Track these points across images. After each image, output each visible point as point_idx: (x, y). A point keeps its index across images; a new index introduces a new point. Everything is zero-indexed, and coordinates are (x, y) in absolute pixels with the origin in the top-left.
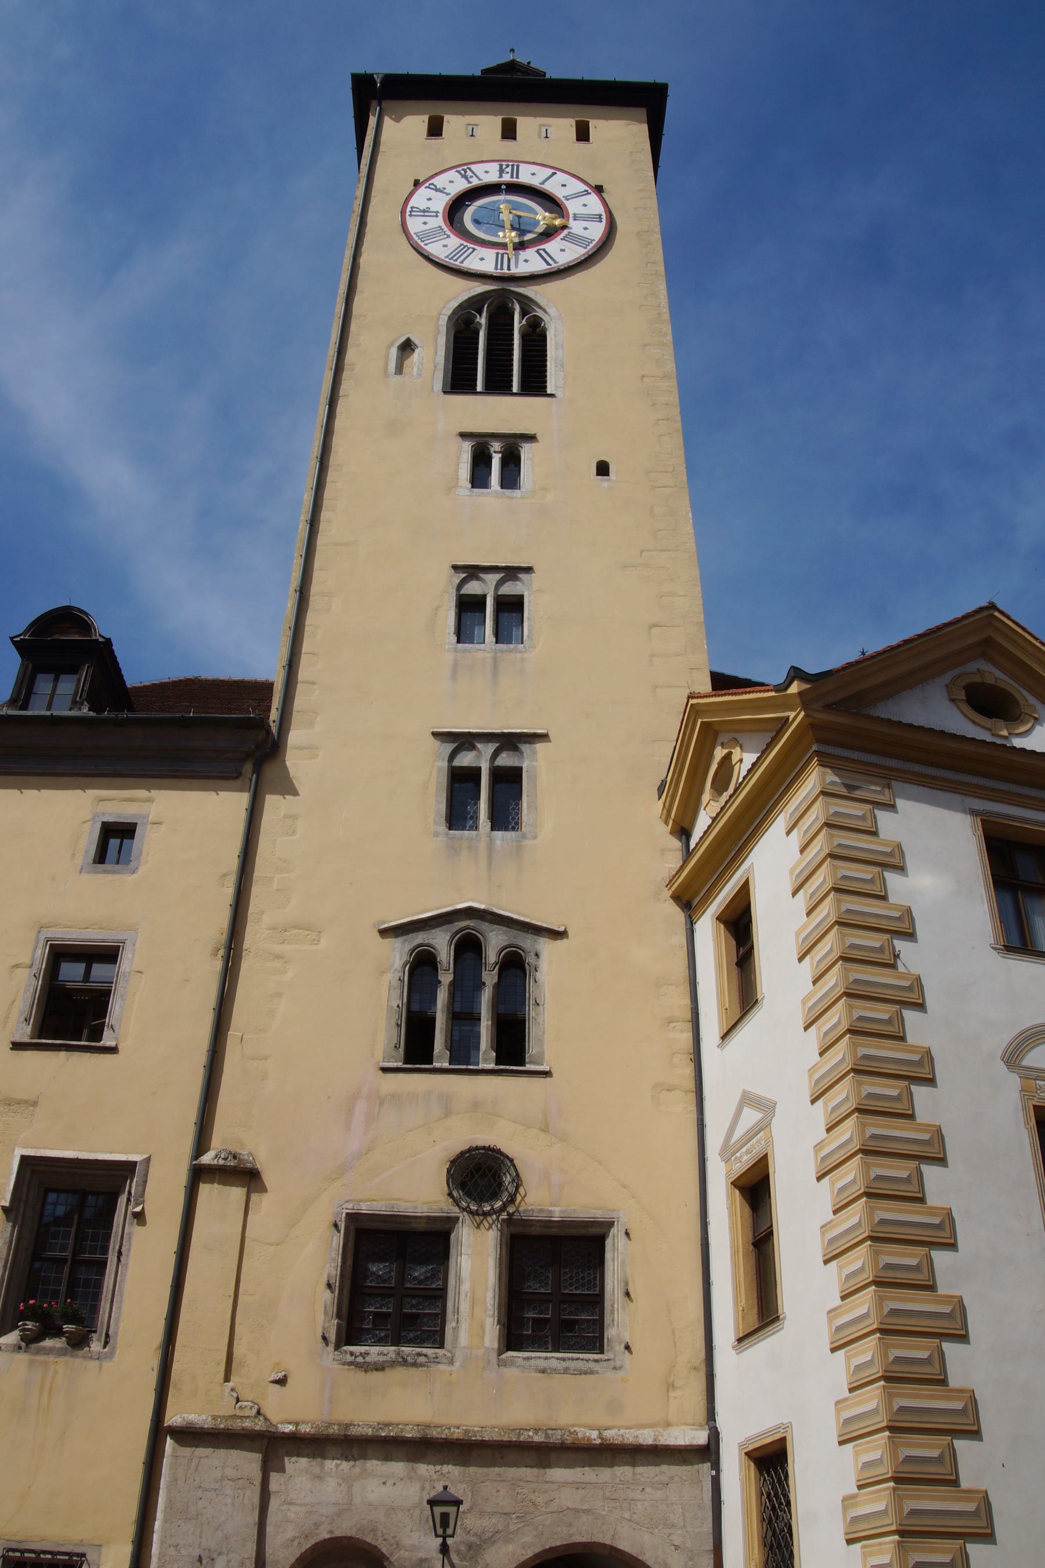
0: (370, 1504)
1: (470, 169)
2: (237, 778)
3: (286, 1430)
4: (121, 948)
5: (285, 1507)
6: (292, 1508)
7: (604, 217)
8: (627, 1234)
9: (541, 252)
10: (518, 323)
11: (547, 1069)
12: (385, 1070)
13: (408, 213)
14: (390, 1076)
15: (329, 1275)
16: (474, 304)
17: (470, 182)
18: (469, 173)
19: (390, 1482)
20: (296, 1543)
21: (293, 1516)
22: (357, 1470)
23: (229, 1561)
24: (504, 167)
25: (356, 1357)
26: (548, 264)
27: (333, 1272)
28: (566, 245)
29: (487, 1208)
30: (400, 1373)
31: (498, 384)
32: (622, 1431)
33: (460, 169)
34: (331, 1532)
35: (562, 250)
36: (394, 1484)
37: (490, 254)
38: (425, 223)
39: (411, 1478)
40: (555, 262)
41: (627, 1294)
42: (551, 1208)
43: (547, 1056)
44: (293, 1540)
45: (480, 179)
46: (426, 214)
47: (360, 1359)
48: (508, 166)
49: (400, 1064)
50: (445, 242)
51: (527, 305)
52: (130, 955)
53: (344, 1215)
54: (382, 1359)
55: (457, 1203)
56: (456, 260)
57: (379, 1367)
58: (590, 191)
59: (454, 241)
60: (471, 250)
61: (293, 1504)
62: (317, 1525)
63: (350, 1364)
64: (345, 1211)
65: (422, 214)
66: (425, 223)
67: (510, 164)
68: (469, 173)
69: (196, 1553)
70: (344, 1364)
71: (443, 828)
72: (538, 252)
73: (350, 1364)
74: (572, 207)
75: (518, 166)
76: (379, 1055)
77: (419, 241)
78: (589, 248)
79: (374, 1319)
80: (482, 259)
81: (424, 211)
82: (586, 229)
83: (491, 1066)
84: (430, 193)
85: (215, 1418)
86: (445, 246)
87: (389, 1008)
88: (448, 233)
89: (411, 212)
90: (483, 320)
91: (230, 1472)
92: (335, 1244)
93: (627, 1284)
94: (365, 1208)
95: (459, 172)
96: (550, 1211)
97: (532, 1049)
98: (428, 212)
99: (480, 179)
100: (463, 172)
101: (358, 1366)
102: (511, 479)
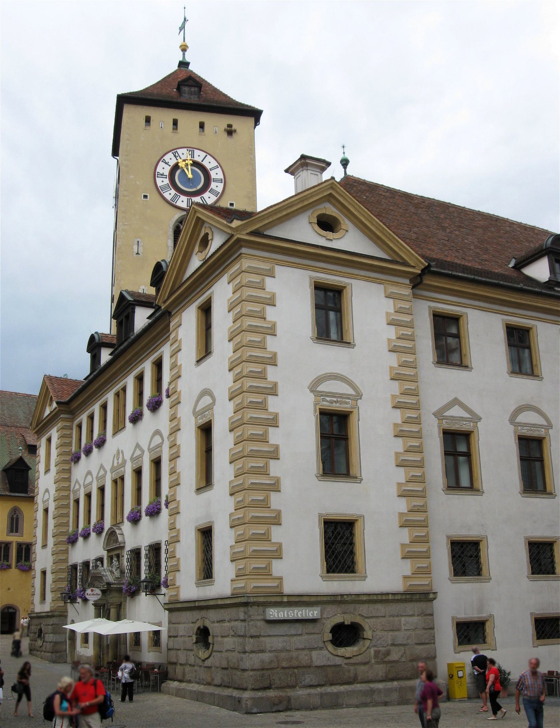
1: (177, 152)
7: (223, 180)
17: (177, 160)
33: (173, 152)
35: (209, 198)
38: (163, 181)
59: (173, 192)
66: (163, 181)
67: (191, 149)
68: (177, 155)
72: (201, 198)
74: (213, 174)
75: (194, 151)
78: (218, 196)
81: (162, 175)
88: (171, 187)
89: (158, 175)
95: (173, 153)
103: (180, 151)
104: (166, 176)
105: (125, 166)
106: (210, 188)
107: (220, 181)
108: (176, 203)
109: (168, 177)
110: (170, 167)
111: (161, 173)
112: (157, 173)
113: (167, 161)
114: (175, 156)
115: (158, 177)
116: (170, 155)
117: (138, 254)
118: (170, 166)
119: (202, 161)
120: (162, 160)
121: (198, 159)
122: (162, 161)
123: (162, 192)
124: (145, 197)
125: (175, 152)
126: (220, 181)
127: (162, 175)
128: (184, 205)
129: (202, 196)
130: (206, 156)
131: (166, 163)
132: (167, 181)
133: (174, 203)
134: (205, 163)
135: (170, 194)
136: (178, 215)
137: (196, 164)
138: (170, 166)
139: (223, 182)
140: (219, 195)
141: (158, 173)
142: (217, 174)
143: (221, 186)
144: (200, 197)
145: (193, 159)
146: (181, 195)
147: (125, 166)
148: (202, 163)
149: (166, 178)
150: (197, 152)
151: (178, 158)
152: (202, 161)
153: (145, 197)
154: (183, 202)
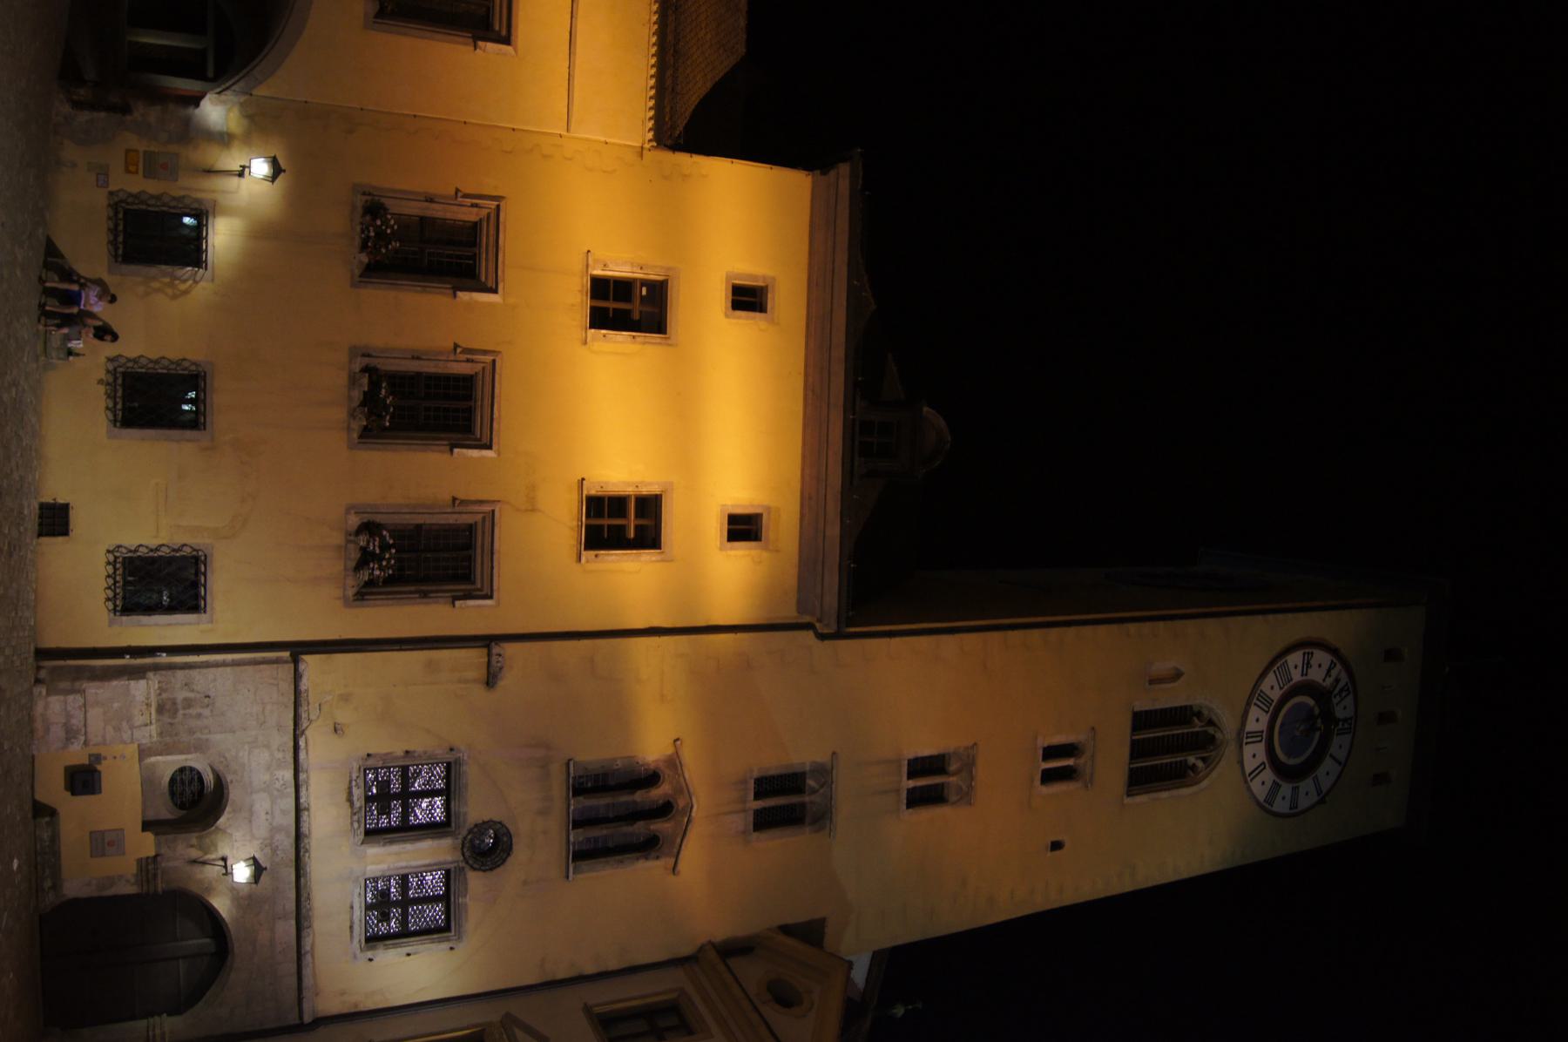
0: (252, 806)
1: (1349, 693)
2: (799, 613)
3: (300, 743)
4: (658, 551)
5: (246, 747)
6: (247, 753)
8: (452, 948)
9: (1263, 767)
11: (570, 878)
12: (568, 765)
14: (564, 769)
15: (414, 752)
18: (1344, 694)
19: (269, 817)
20: (222, 759)
21: (241, 754)
22: (275, 793)
23: (207, 718)
24: (1349, 721)
25: (356, 781)
26: (1250, 775)
27: (416, 755)
28: (1269, 784)
29: (467, 854)
30: (346, 810)
31: (1137, 750)
32: (311, 965)
34: (232, 782)
35: (1263, 783)
36: (267, 820)
37: (1263, 725)
38: (1296, 667)
39: (271, 830)
40: (1251, 780)
41: (409, 955)
42: (468, 897)
43: (579, 876)
44: (224, 757)
45: (1337, 704)
47: (354, 783)
48: (1350, 724)
49: (572, 775)
50: (1276, 687)
52: (654, 558)
53: (458, 755)
54: (355, 798)
55: (470, 831)
56: (1258, 699)
57: (350, 800)
58: (1321, 795)
59: (1276, 695)
60: (1266, 709)
61: (249, 754)
62: (235, 772)
63: (350, 776)
64: (461, 755)
65: (1306, 661)
66: (1296, 667)
68: (1344, 694)
69: (210, 694)
70: (350, 773)
71: (756, 774)
72: (1263, 763)
73: (350, 776)
74: (1307, 785)
76: (578, 758)
77: (1279, 665)
79: (385, 781)
80: (1257, 720)
81: (1308, 663)
82: (1284, 798)
83: (572, 839)
84: (1325, 667)
85: (307, 691)
86: (1272, 688)
87: (615, 760)
91: (269, 707)
92: (437, 752)
93: (415, 953)
94: (464, 768)
96: (465, 896)
97: (584, 864)
98: (1307, 667)
99: (1337, 704)
100: (1346, 688)
101: (351, 782)
102: (1049, 777)
103: (1349, 700)
108: (1255, 704)
109: (1304, 678)
110: (1321, 681)
111: (1312, 662)
115: (1304, 654)
119: (1331, 756)
122: (1332, 661)
123: (1275, 668)
128: (1251, 726)
130: (1340, 763)
131: (1329, 671)
132: (1297, 676)
133: (1255, 700)
138: (1324, 680)
141: (1312, 653)
146: (1269, 714)
148: (1328, 756)
149: (1302, 675)
151: (1338, 698)
152: (1331, 756)
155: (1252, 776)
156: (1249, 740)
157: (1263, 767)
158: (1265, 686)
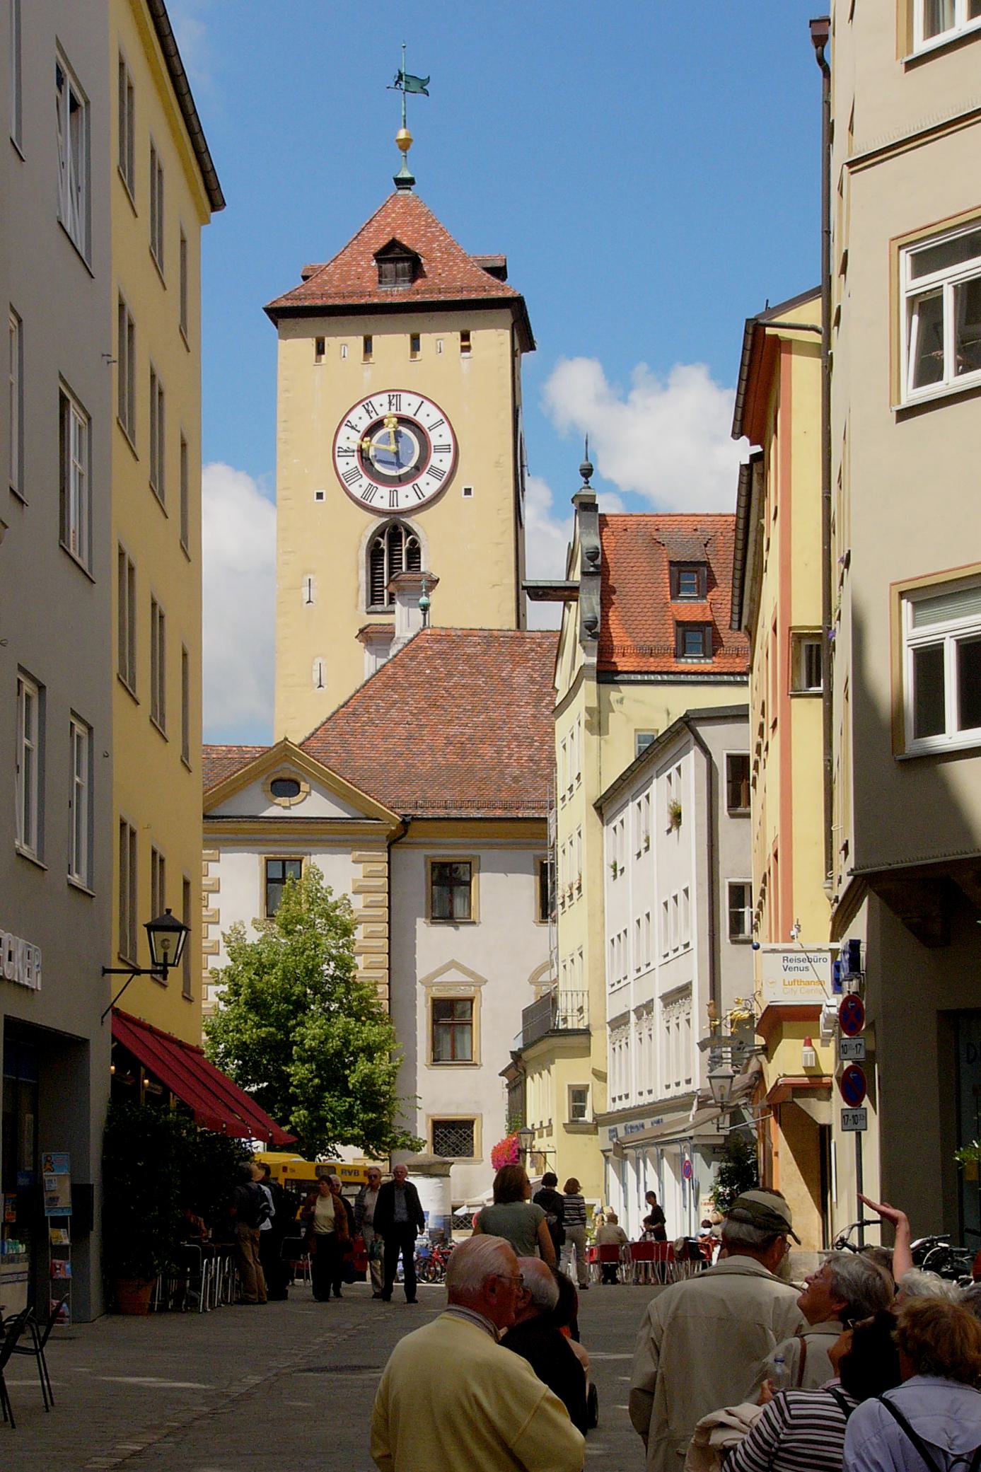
7: (452, 447)
9: (415, 487)
10: (405, 545)
13: (337, 454)
16: (380, 532)
17: (371, 418)
46: (348, 454)
51: (409, 532)
59: (366, 481)
65: (344, 454)
67: (395, 393)
68: (371, 408)
74: (434, 439)
81: (346, 451)
88: (361, 472)
90: (384, 544)
104: (353, 451)
105: (285, 442)
106: (429, 466)
107: (445, 449)
112: (337, 450)
113: (353, 424)
114: (368, 411)
116: (360, 410)
117: (309, 602)
118: (359, 432)
119: (415, 415)
120: (345, 422)
121: (407, 412)
122: (346, 425)
124: (320, 496)
125: (367, 404)
126: (445, 449)
127: (346, 451)
129: (415, 482)
131: (352, 427)
134: (421, 419)
135: (360, 486)
136: (376, 522)
137: (403, 420)
138: (359, 432)
139: (452, 450)
140: (445, 477)
142: (440, 437)
143: (448, 458)
144: (412, 484)
145: (398, 412)
147: (285, 442)
150: (406, 398)
151: (373, 415)
152: (415, 415)
153: (320, 496)
154: (382, 498)
155: (421, 496)
156: (395, 504)
157: (415, 487)
158: (357, 492)
